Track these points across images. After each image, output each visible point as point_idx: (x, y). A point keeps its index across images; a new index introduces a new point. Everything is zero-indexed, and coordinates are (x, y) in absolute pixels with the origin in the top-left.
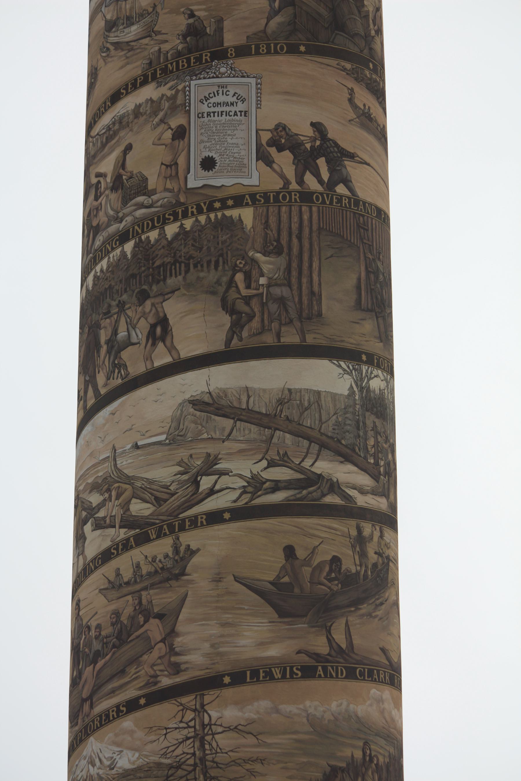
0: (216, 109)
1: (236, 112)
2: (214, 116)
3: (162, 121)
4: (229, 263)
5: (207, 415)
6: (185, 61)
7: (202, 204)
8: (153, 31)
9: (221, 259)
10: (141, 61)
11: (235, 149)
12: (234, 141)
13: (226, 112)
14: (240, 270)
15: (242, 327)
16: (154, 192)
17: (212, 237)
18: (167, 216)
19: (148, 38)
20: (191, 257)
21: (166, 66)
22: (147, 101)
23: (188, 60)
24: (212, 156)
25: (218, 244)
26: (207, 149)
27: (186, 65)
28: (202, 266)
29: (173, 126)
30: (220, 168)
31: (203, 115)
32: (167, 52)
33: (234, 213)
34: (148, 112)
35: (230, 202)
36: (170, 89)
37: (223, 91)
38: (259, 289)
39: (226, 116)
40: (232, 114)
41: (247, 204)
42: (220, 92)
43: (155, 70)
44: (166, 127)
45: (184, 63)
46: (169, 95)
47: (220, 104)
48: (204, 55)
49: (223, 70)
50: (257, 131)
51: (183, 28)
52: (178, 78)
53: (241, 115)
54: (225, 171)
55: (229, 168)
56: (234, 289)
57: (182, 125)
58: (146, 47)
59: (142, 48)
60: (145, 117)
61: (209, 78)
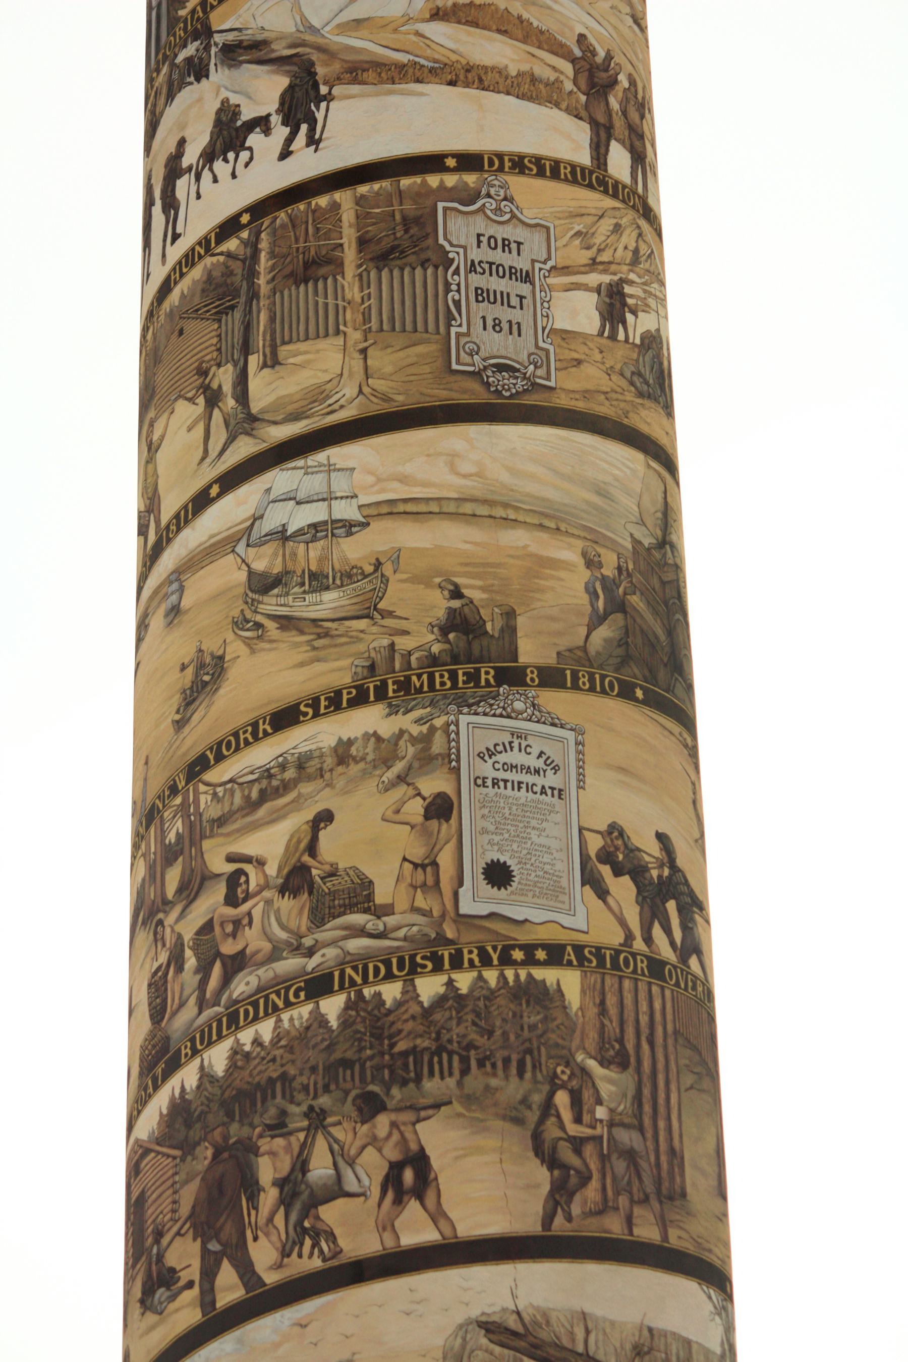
0: (508, 775)
1: (543, 787)
2: (506, 788)
3: (401, 779)
4: (544, 1068)
5: (515, 1356)
6: (446, 675)
7: (490, 949)
8: (375, 609)
9: (528, 1059)
10: (350, 661)
11: (546, 855)
12: (542, 840)
13: (527, 784)
14: (563, 1086)
15: (571, 1195)
16: (388, 910)
17: (510, 1014)
18: (418, 959)
19: (366, 620)
20: (471, 1046)
21: (408, 678)
22: (367, 736)
23: (453, 676)
24: (505, 863)
25: (522, 1028)
26: (496, 848)
27: (449, 684)
28: (494, 1066)
29: (426, 793)
30: (520, 886)
31: (484, 782)
32: (409, 652)
33: (548, 975)
34: (370, 758)
35: (541, 955)
36: (417, 721)
37: (520, 744)
38: (594, 1128)
39: (527, 791)
40: (538, 789)
41: (570, 963)
42: (516, 745)
43: (384, 683)
44: (411, 791)
45: (445, 679)
46: (415, 734)
47: (516, 767)
48: (483, 670)
49: (519, 705)
50: (581, 830)
51: (440, 613)
52: (432, 704)
53: (553, 796)
54: (530, 894)
55: (537, 890)
56: (553, 1119)
57: (445, 793)
58: (362, 635)
59: (351, 637)
60: (362, 765)
61: (494, 715)
